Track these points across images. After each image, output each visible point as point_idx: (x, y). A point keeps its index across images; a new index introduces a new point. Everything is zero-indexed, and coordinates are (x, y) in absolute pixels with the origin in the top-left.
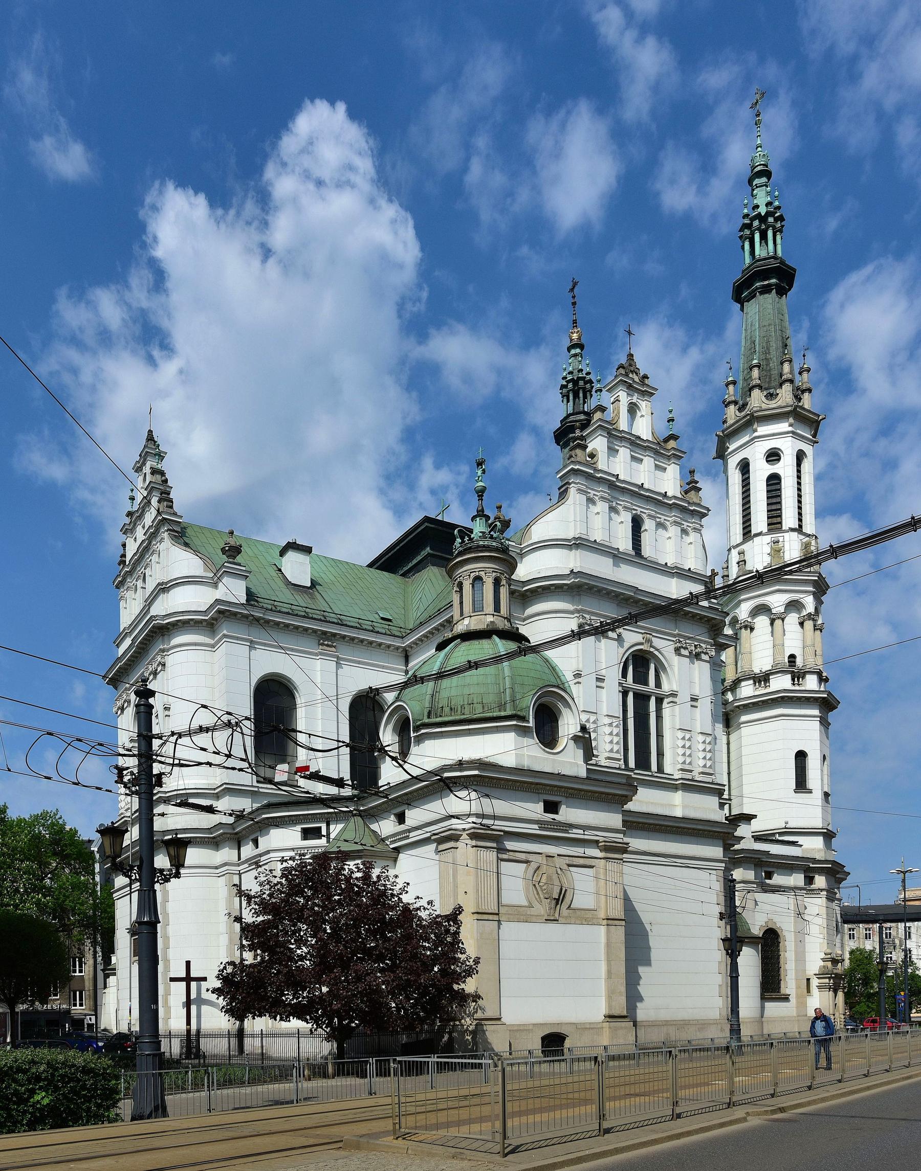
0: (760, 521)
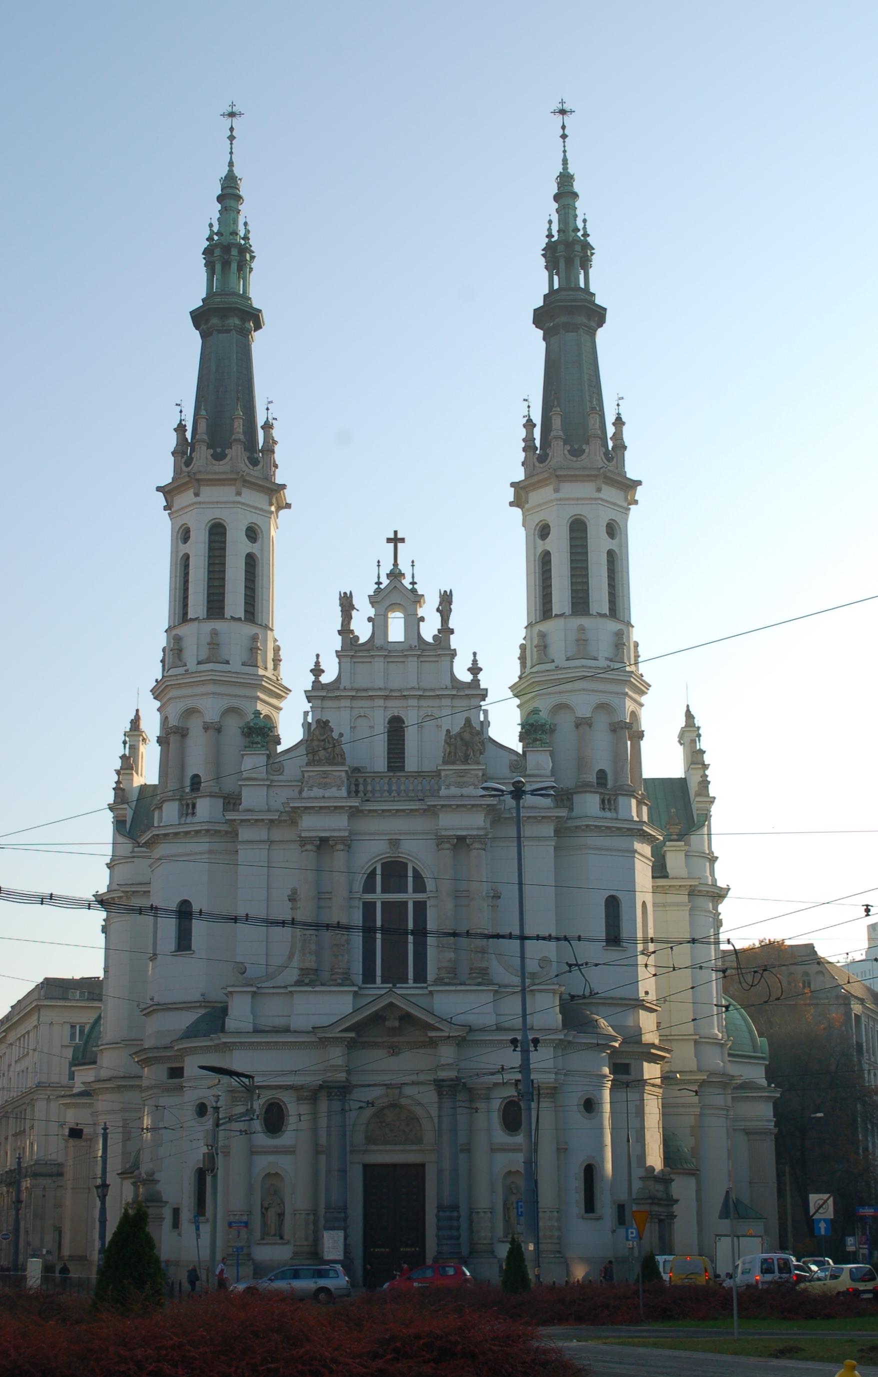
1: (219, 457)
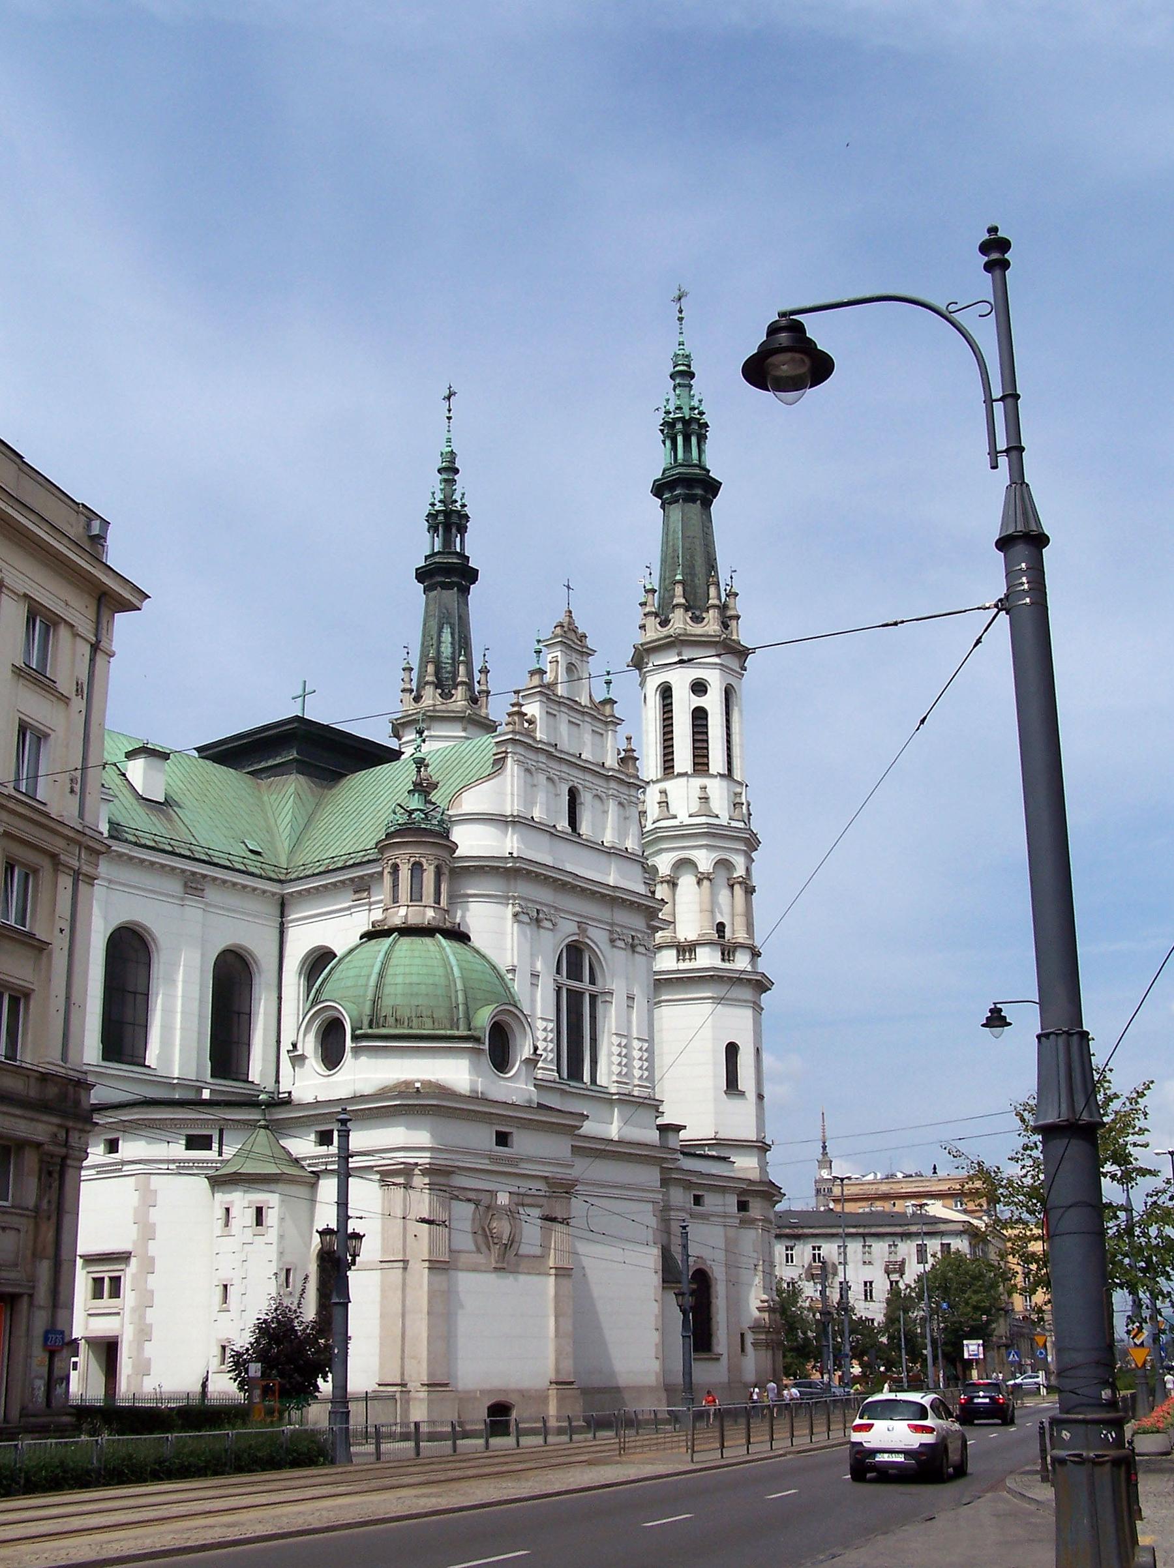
0: (683, 758)
1: (697, 619)
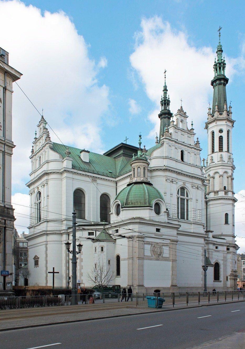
1: (221, 114)
